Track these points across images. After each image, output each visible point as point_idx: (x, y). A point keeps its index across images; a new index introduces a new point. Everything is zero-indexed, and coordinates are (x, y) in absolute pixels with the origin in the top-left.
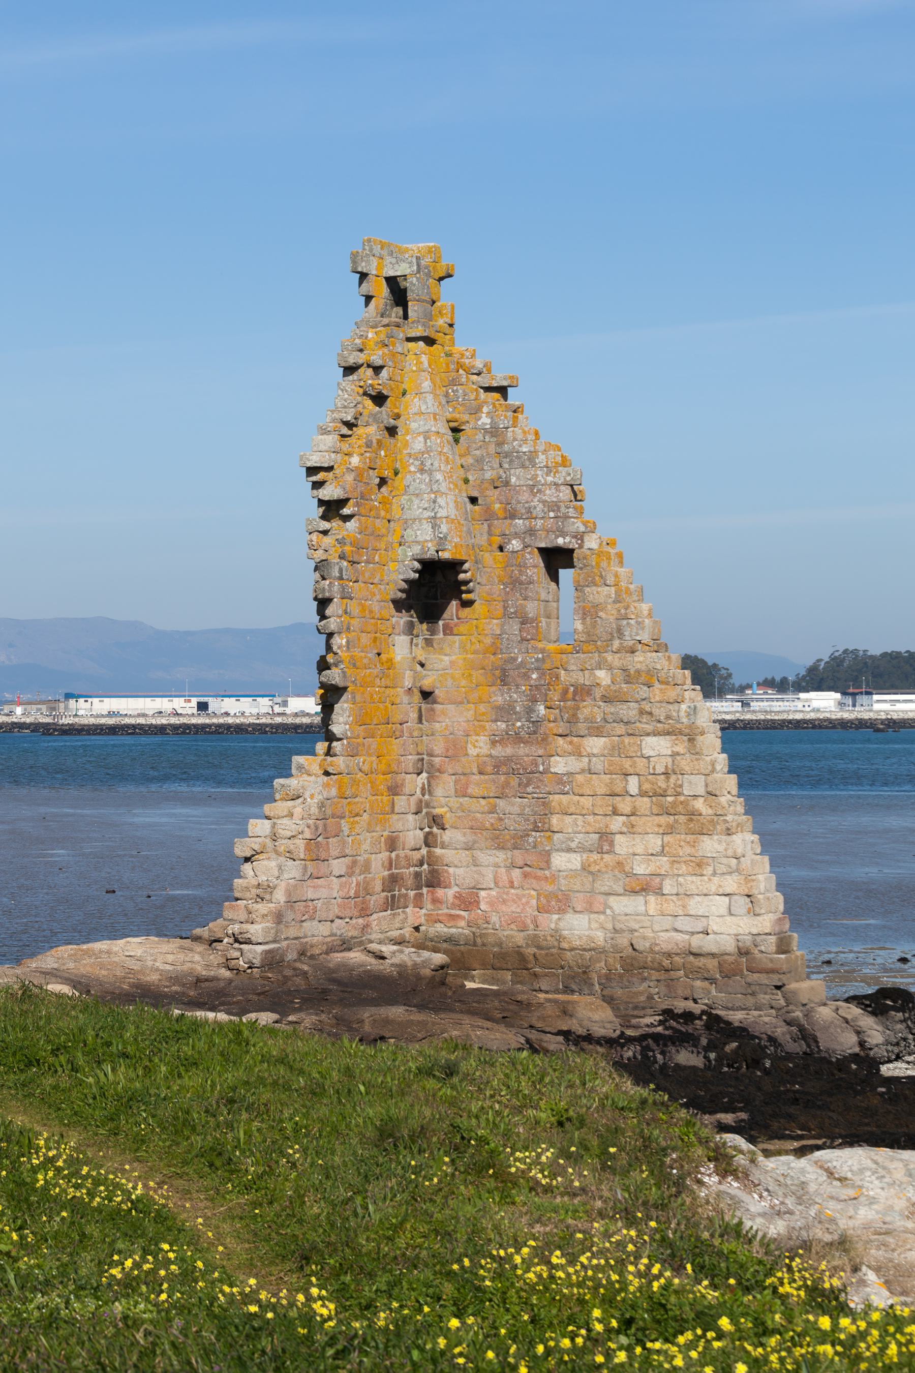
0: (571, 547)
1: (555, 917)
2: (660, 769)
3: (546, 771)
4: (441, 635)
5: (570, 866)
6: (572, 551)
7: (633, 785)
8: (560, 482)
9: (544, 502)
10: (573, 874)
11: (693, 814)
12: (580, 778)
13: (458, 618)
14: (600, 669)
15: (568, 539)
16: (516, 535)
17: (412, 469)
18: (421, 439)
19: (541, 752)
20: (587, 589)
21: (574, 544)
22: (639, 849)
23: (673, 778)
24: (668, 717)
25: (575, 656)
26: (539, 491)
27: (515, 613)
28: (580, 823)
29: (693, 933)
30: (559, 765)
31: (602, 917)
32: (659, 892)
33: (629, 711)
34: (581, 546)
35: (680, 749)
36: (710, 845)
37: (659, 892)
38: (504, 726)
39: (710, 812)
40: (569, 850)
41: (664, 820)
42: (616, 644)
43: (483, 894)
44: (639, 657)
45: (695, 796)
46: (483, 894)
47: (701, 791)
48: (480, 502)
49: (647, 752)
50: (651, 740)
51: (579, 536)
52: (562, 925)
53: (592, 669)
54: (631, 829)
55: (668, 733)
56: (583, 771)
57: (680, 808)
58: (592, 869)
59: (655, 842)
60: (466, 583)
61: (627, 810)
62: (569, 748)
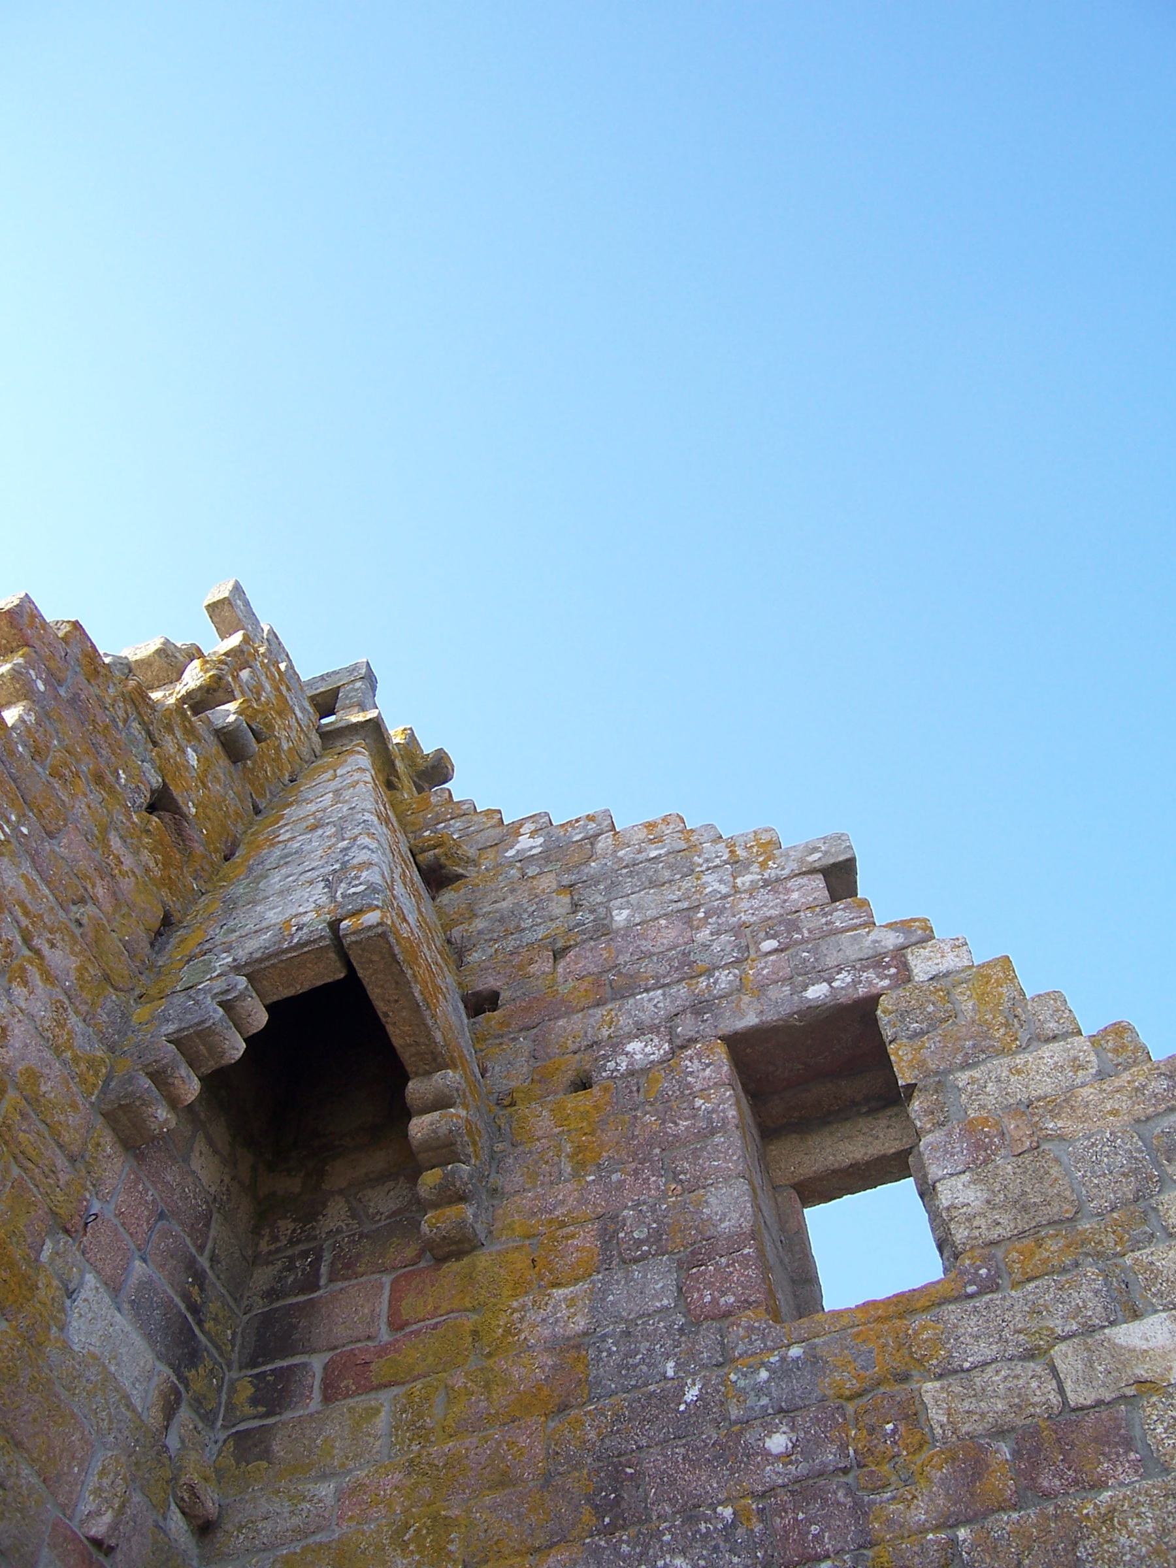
0: (862, 991)
4: (315, 1403)
6: (872, 1001)
8: (786, 872)
13: (397, 1324)
14: (1136, 1315)
15: (843, 979)
16: (641, 1031)
25: (979, 1302)
27: (656, 1237)
48: (505, 995)
53: (1090, 1330)
60: (445, 1150)
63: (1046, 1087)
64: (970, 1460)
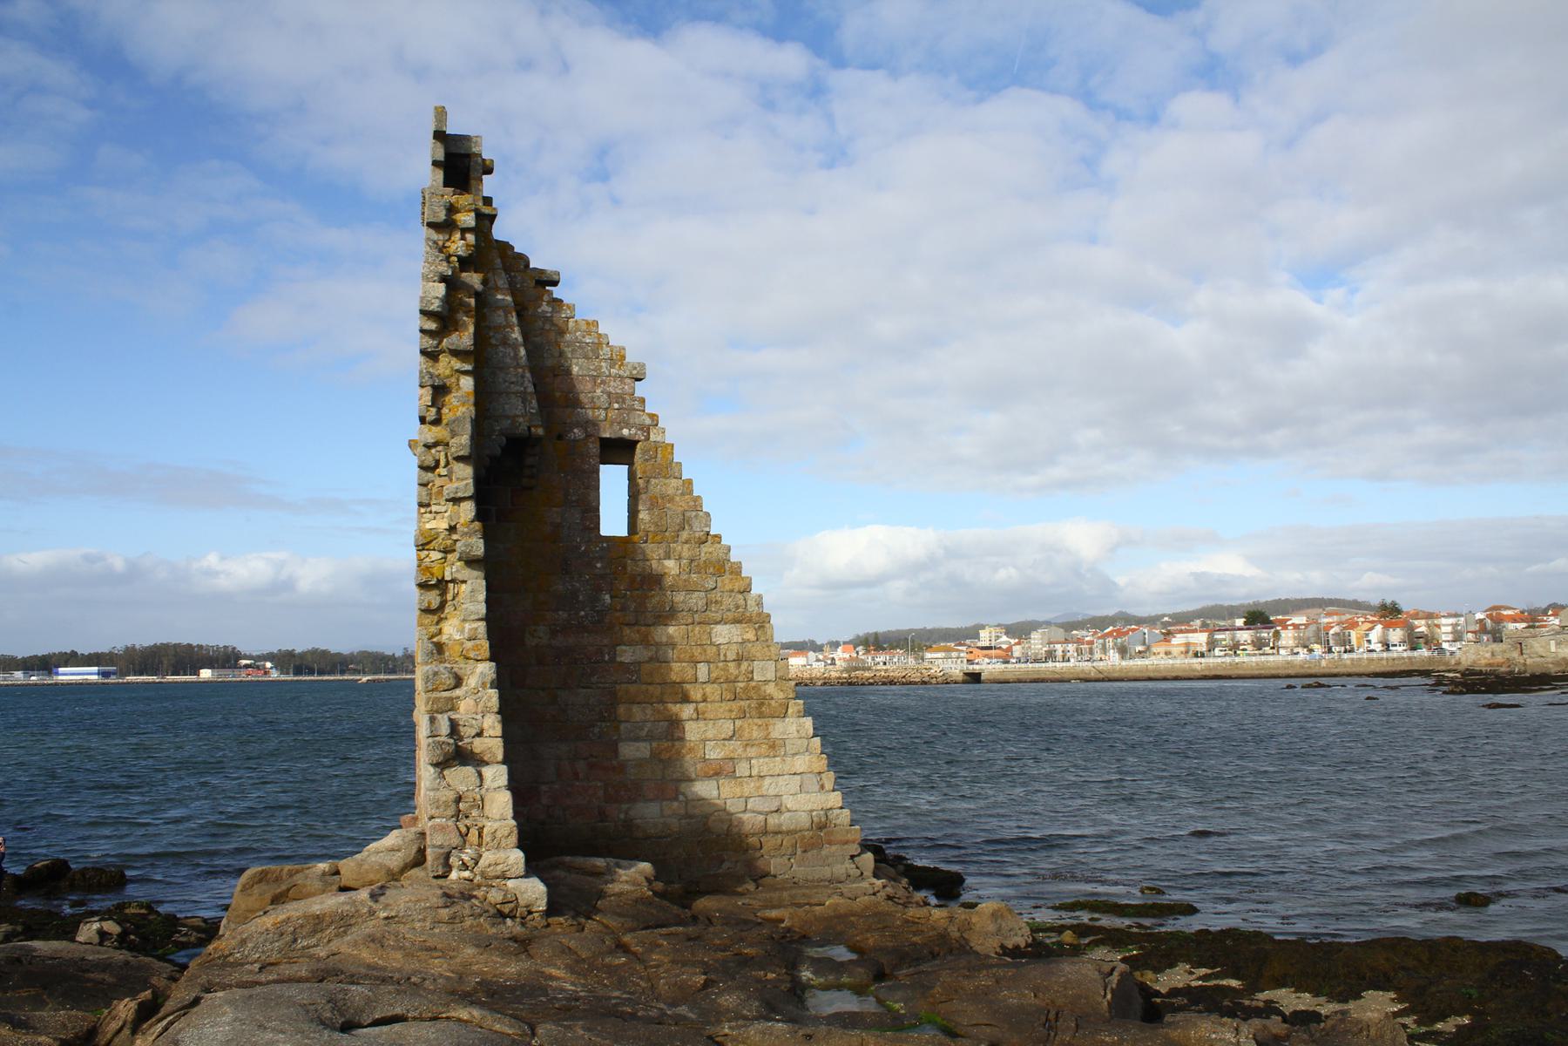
1: (625, 806)
2: (731, 656)
3: (612, 660)
5: (638, 755)
7: (702, 671)
9: (609, 394)
10: (640, 763)
11: (763, 700)
12: (647, 667)
15: (633, 431)
17: (493, 341)
18: (501, 312)
19: (605, 642)
20: (653, 481)
21: (640, 436)
22: (710, 735)
23: (745, 665)
24: (737, 607)
26: (603, 382)
28: (649, 712)
29: (767, 814)
30: (626, 655)
31: (675, 804)
32: (732, 775)
33: (697, 600)
34: (648, 438)
35: (750, 635)
36: (779, 729)
37: (732, 775)
38: (563, 615)
39: (781, 695)
40: (637, 739)
41: (735, 705)
42: (684, 535)
43: (544, 788)
44: (705, 548)
45: (766, 682)
46: (544, 788)
47: (770, 675)
49: (720, 640)
50: (719, 627)
51: (646, 430)
52: (632, 813)
54: (699, 716)
55: (739, 622)
56: (651, 659)
57: (752, 693)
58: (665, 756)
59: (727, 727)
61: (699, 697)
62: (636, 637)
63: (670, 492)
64: (633, 579)
